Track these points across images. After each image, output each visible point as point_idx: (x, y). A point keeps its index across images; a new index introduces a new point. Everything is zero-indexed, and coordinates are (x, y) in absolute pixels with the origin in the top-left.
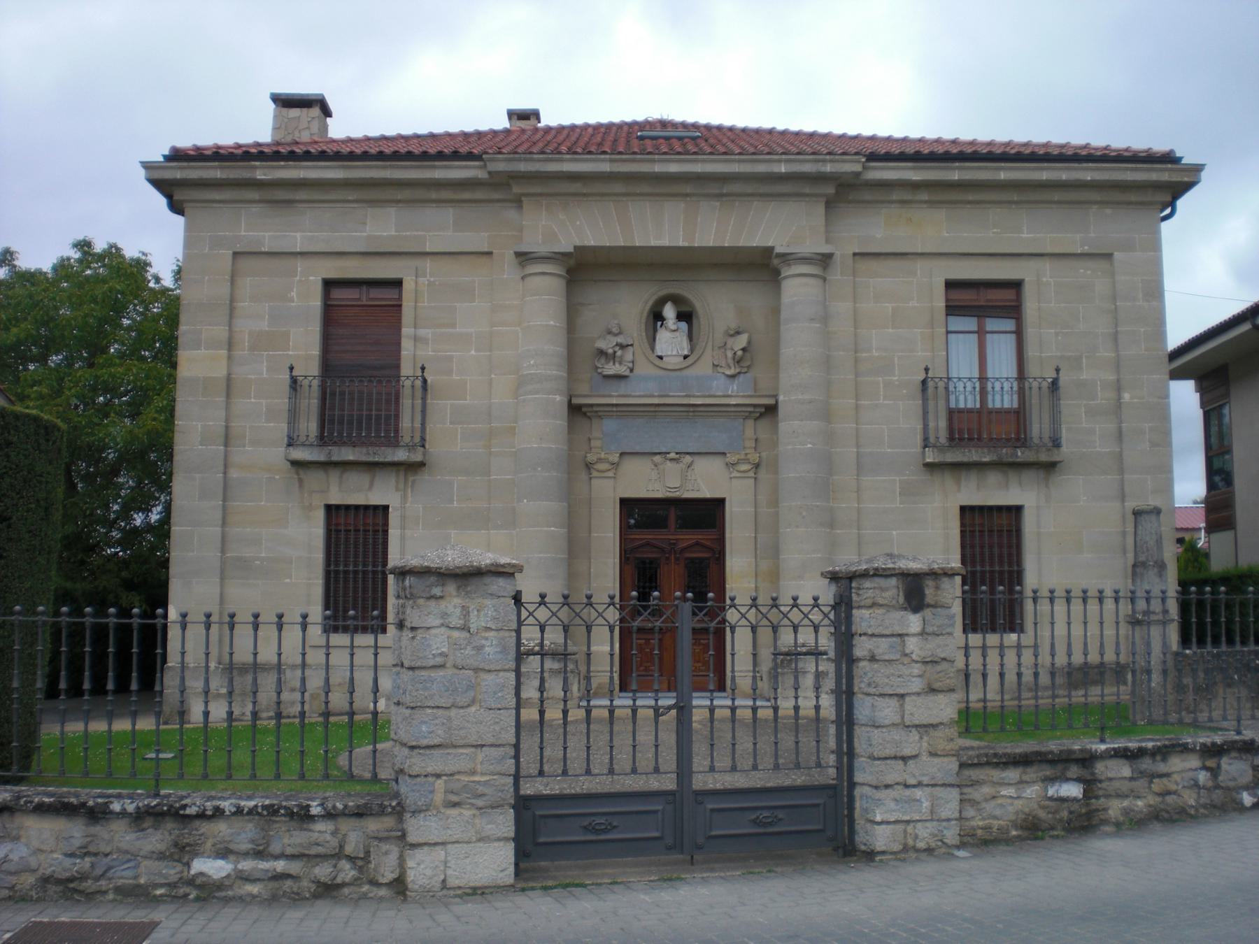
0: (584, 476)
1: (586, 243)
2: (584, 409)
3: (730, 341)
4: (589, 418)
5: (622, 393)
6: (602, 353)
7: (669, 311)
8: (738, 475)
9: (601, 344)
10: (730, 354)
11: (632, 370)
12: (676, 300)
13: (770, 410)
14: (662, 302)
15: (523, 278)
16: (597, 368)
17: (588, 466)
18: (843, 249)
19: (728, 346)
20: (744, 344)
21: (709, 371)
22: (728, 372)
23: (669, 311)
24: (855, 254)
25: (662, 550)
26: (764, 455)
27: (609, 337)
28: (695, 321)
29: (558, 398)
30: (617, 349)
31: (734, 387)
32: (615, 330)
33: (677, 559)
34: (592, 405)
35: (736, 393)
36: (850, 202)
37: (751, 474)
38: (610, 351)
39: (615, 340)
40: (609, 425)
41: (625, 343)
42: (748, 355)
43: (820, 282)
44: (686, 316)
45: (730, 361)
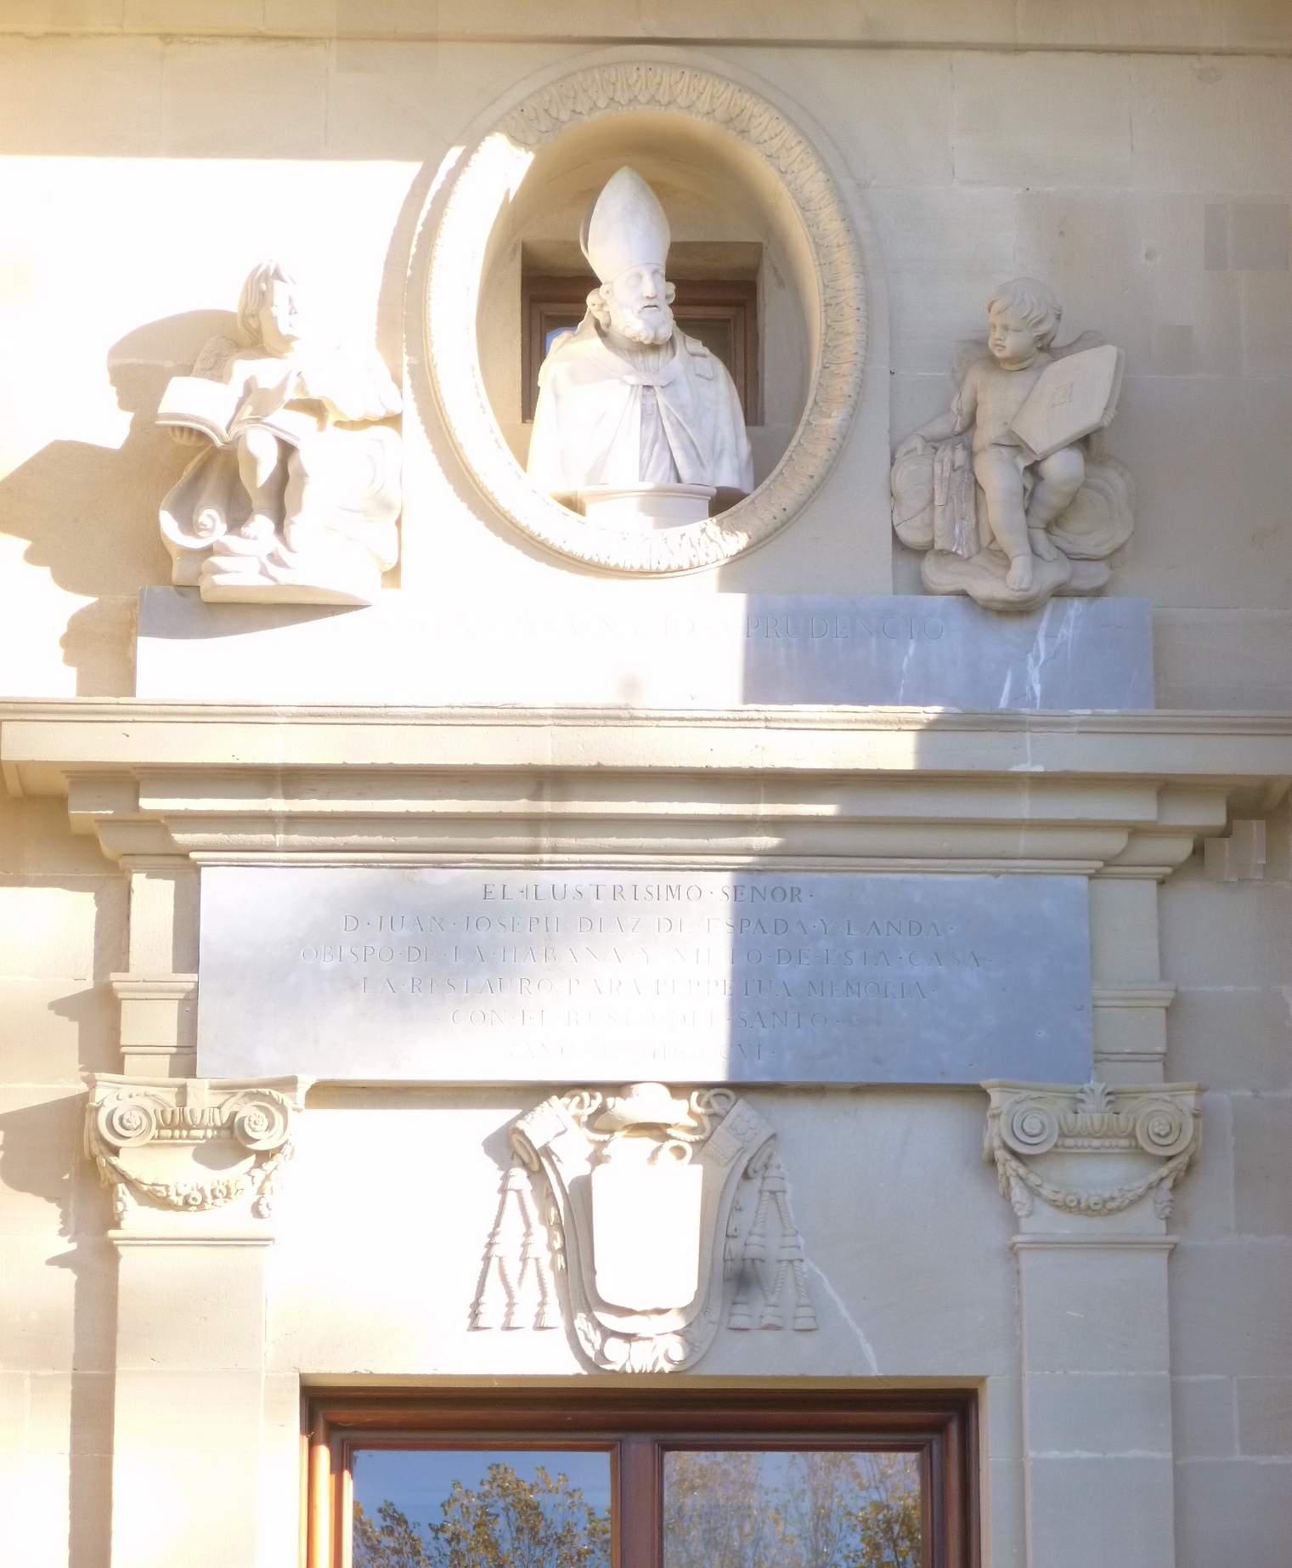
2: (84, 812)
3: (998, 401)
8: (1068, 1227)
10: (998, 478)
12: (676, 166)
19: (988, 431)
20: (1089, 413)
21: (877, 569)
22: (987, 588)
34: (130, 780)
37: (1146, 1221)
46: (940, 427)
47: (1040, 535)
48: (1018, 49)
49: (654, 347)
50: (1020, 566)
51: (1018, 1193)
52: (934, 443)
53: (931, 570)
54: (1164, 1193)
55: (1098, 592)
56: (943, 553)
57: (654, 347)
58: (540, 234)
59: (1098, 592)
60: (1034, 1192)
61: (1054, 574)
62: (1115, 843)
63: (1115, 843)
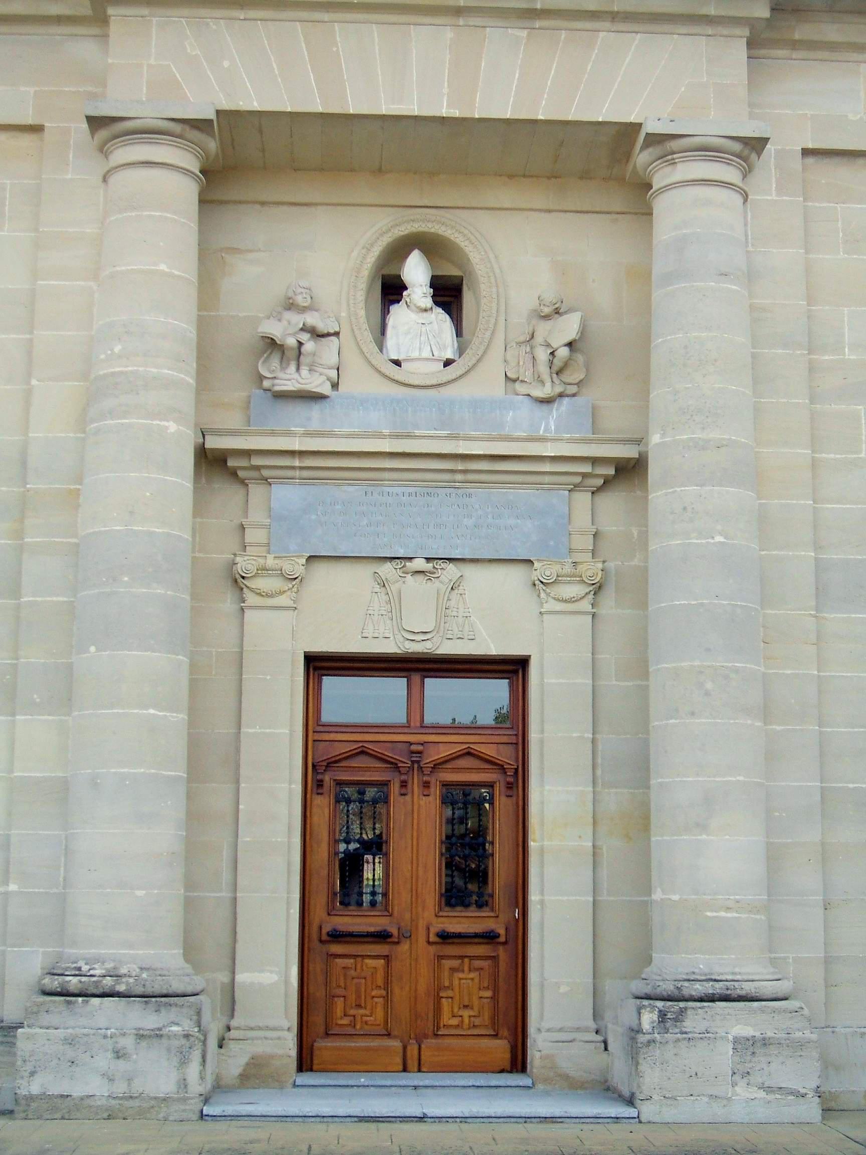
0: (228, 604)
1: (243, 105)
2: (230, 463)
3: (543, 329)
4: (243, 483)
5: (315, 426)
6: (272, 345)
7: (416, 272)
8: (559, 607)
9: (274, 329)
10: (542, 355)
11: (335, 386)
13: (629, 471)
14: (399, 250)
15: (105, 179)
16: (261, 378)
17: (237, 582)
18: (787, 140)
19: (539, 339)
22: (539, 393)
23: (416, 272)
24: (807, 152)
25: (395, 766)
26: (611, 565)
27: (288, 315)
28: (467, 297)
29: (172, 427)
30: (304, 337)
31: (551, 421)
32: (300, 300)
33: (426, 785)
34: (248, 453)
35: (556, 433)
36: (795, 45)
37: (586, 605)
38: (291, 342)
39: (298, 320)
40: (286, 495)
41: (322, 327)
42: (580, 358)
43: (738, 199)
44: (448, 294)
45: (543, 369)
46: (522, 339)
47: (555, 376)
48: (549, 211)
49: (426, 310)
50: (548, 384)
51: (543, 595)
52: (519, 344)
53: (517, 385)
54: (591, 596)
55: (574, 395)
56: (522, 381)
57: (426, 310)
58: (387, 271)
59: (574, 395)
60: (548, 595)
61: (559, 389)
62: (578, 479)
63: (578, 479)
